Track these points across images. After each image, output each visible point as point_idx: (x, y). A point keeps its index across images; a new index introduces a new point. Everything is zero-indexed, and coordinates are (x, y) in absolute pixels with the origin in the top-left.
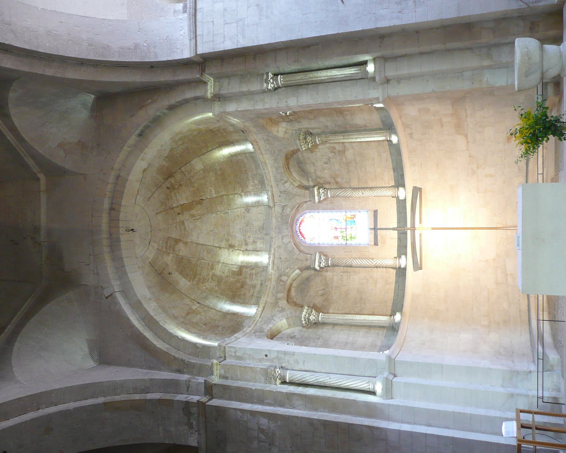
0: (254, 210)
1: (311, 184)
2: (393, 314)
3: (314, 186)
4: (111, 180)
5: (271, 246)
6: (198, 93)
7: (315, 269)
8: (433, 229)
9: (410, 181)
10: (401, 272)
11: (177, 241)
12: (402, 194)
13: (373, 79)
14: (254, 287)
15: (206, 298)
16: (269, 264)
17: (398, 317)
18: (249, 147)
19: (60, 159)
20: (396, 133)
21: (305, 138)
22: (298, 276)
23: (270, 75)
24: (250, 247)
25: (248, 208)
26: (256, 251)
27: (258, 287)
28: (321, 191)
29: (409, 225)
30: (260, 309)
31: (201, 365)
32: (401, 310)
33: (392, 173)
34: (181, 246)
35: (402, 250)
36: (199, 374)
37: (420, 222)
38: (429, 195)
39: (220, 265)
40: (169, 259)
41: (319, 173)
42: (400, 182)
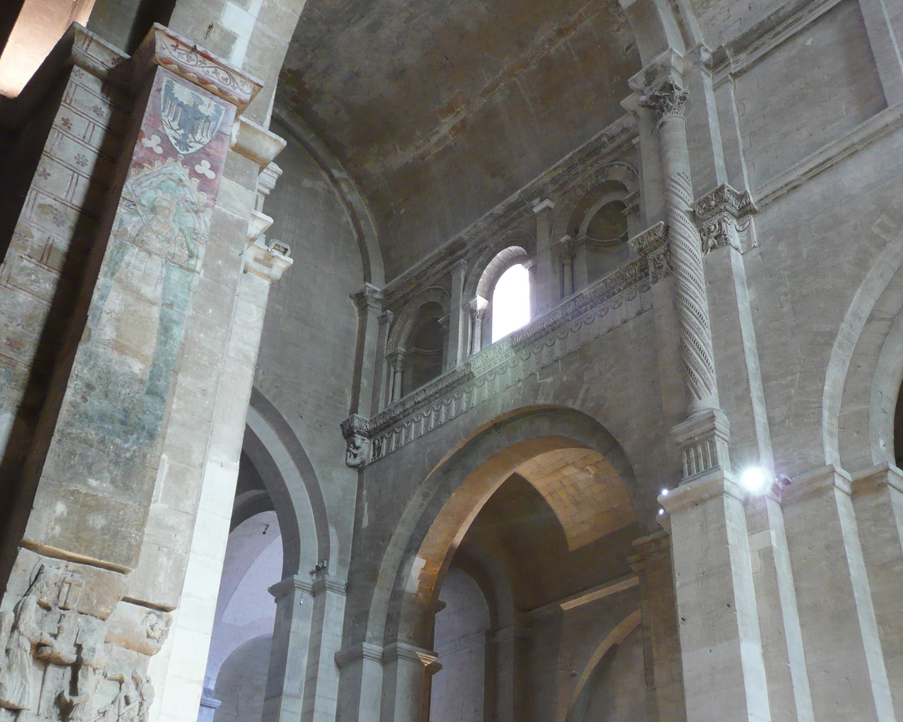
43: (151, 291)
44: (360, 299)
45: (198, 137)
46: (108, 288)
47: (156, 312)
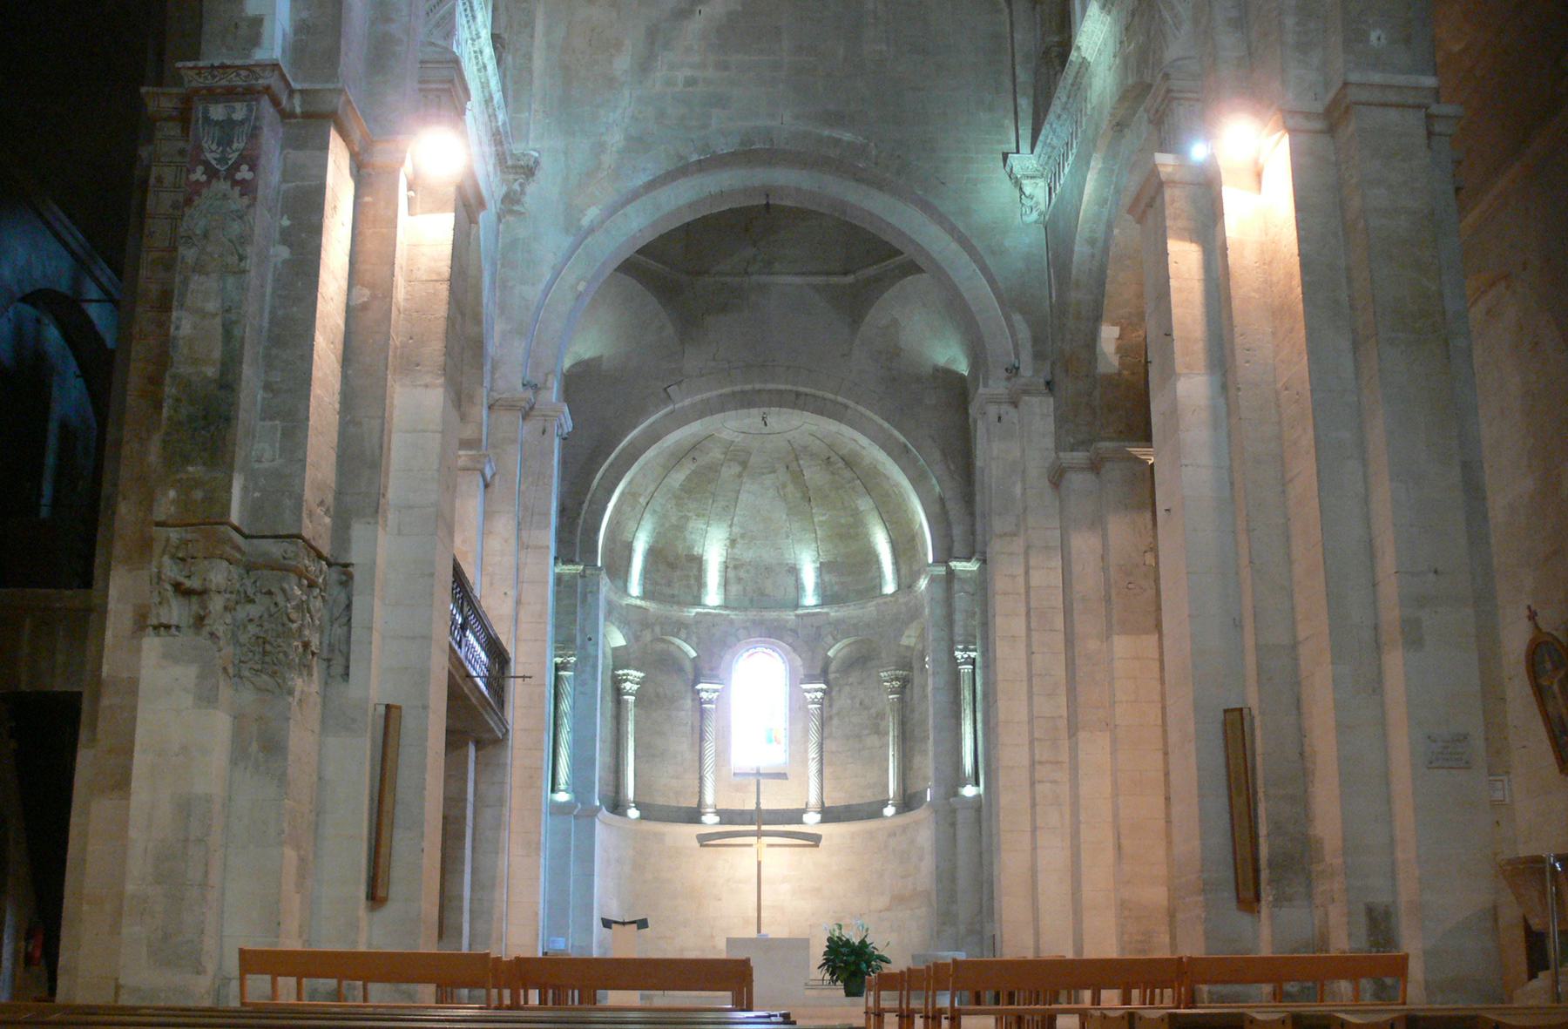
0: (791, 581)
1: (831, 676)
3: (826, 682)
5: (734, 609)
6: (958, 547)
7: (696, 682)
8: (759, 864)
9: (827, 830)
10: (694, 816)
11: (744, 464)
12: (812, 820)
13: (956, 794)
16: (705, 606)
17: (633, 813)
18: (889, 587)
19: (876, 317)
20: (898, 813)
21: (897, 679)
24: (731, 574)
25: (794, 571)
26: (726, 584)
27: (668, 591)
28: (820, 695)
29: (764, 828)
30: (639, 602)
31: (574, 544)
32: (642, 817)
34: (736, 469)
35: (727, 816)
38: (808, 858)
40: (716, 454)
41: (847, 689)
42: (830, 815)
43: (212, 306)
45: (235, 146)
46: (179, 319)
47: (218, 320)
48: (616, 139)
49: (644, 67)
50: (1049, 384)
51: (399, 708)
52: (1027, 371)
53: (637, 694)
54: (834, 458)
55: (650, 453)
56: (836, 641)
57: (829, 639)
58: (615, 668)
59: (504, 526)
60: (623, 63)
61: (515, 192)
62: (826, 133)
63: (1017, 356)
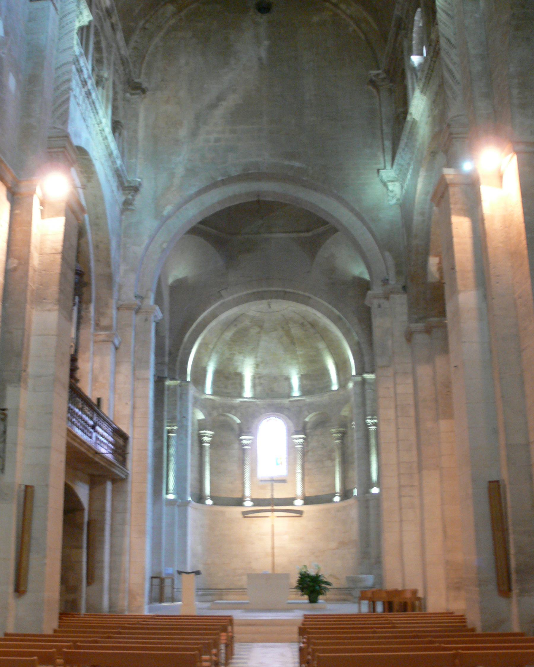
1: (308, 431)
2: (212, 498)
4: (307, 294)
9: (309, 509)
10: (239, 502)
11: (261, 327)
14: (226, 387)
15: (217, 352)
17: (209, 502)
18: (335, 387)
19: (323, 253)
21: (340, 432)
22: (235, 421)
23: (376, 421)
24: (257, 381)
25: (288, 379)
26: (254, 386)
28: (302, 440)
32: (215, 504)
33: (315, 495)
34: (257, 329)
35: (257, 502)
36: (170, 369)
37: (278, 517)
38: (298, 523)
39: (242, 358)
40: (247, 323)
42: (308, 501)
44: (372, 82)
48: (180, 171)
49: (194, 134)
50: (404, 288)
51: (32, 487)
52: (392, 282)
53: (211, 443)
54: (306, 323)
55: (213, 324)
56: (310, 413)
57: (306, 413)
58: (200, 430)
59: (126, 369)
60: (183, 132)
61: (129, 199)
62: (286, 163)
63: (388, 274)
